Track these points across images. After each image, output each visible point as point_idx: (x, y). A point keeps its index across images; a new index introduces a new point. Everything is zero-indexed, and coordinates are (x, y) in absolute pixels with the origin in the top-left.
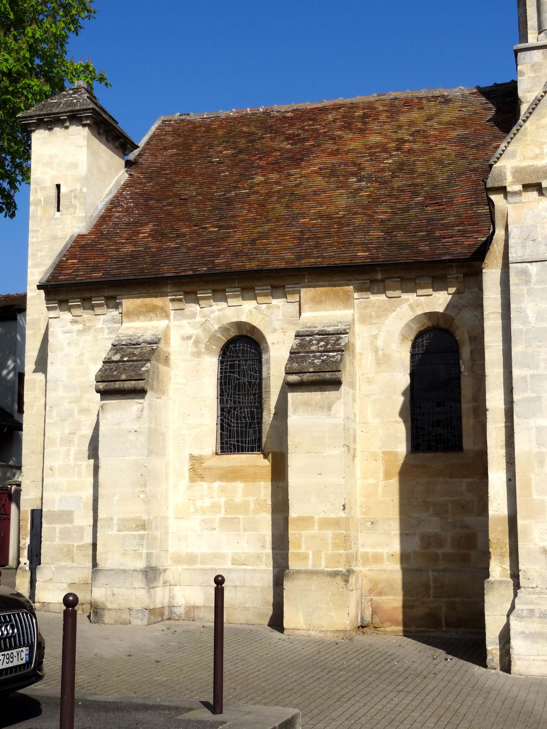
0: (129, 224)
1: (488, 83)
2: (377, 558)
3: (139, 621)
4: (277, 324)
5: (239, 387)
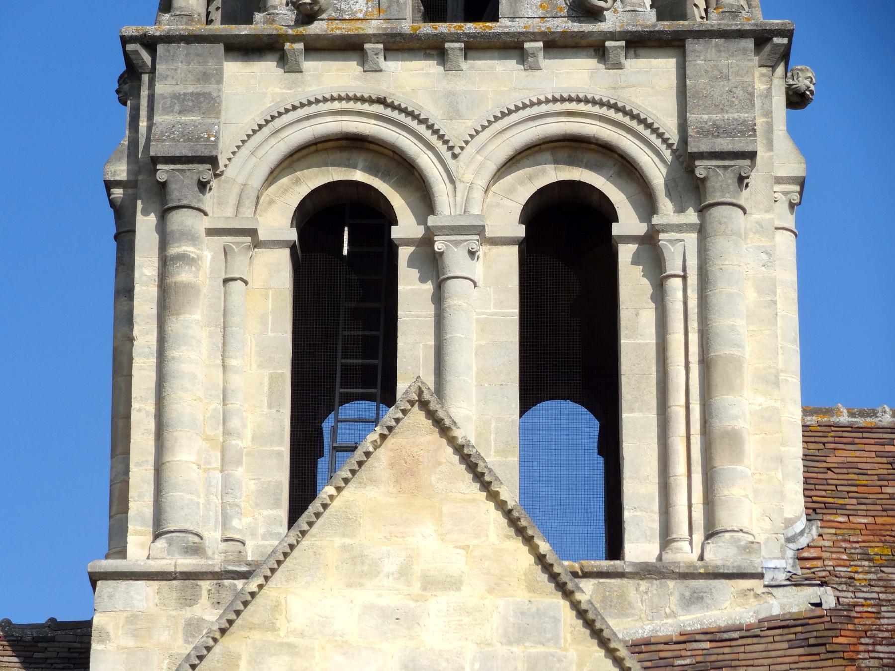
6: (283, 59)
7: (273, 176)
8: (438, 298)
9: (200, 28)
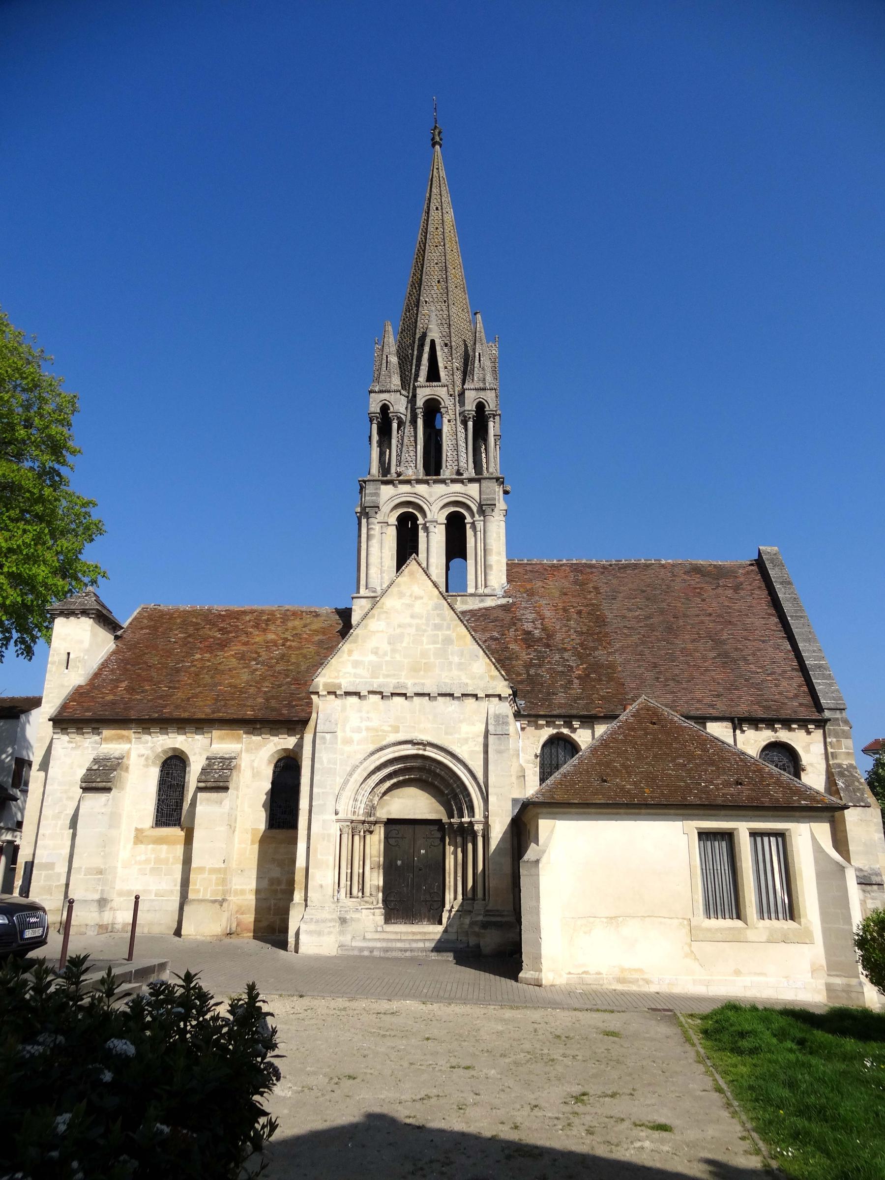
0: (112, 680)
1: (342, 606)
2: (243, 892)
3: (91, 933)
4: (197, 751)
5: (171, 786)
6: (394, 485)
7: (392, 510)
8: (428, 536)
9: (377, 478)
